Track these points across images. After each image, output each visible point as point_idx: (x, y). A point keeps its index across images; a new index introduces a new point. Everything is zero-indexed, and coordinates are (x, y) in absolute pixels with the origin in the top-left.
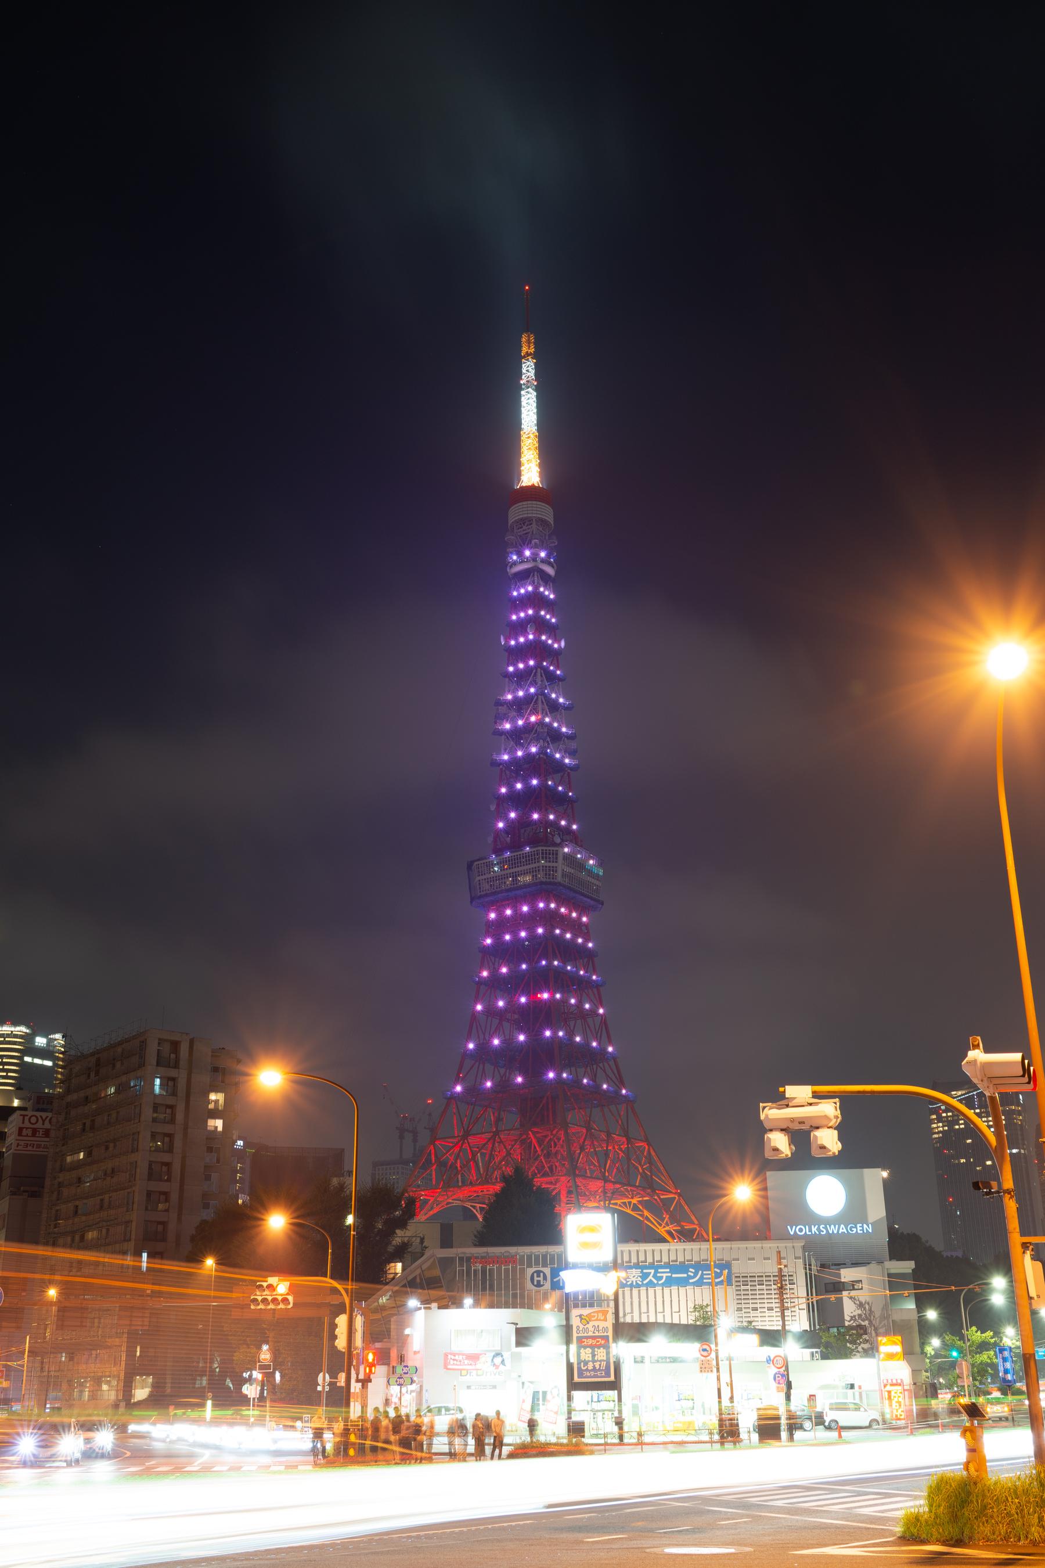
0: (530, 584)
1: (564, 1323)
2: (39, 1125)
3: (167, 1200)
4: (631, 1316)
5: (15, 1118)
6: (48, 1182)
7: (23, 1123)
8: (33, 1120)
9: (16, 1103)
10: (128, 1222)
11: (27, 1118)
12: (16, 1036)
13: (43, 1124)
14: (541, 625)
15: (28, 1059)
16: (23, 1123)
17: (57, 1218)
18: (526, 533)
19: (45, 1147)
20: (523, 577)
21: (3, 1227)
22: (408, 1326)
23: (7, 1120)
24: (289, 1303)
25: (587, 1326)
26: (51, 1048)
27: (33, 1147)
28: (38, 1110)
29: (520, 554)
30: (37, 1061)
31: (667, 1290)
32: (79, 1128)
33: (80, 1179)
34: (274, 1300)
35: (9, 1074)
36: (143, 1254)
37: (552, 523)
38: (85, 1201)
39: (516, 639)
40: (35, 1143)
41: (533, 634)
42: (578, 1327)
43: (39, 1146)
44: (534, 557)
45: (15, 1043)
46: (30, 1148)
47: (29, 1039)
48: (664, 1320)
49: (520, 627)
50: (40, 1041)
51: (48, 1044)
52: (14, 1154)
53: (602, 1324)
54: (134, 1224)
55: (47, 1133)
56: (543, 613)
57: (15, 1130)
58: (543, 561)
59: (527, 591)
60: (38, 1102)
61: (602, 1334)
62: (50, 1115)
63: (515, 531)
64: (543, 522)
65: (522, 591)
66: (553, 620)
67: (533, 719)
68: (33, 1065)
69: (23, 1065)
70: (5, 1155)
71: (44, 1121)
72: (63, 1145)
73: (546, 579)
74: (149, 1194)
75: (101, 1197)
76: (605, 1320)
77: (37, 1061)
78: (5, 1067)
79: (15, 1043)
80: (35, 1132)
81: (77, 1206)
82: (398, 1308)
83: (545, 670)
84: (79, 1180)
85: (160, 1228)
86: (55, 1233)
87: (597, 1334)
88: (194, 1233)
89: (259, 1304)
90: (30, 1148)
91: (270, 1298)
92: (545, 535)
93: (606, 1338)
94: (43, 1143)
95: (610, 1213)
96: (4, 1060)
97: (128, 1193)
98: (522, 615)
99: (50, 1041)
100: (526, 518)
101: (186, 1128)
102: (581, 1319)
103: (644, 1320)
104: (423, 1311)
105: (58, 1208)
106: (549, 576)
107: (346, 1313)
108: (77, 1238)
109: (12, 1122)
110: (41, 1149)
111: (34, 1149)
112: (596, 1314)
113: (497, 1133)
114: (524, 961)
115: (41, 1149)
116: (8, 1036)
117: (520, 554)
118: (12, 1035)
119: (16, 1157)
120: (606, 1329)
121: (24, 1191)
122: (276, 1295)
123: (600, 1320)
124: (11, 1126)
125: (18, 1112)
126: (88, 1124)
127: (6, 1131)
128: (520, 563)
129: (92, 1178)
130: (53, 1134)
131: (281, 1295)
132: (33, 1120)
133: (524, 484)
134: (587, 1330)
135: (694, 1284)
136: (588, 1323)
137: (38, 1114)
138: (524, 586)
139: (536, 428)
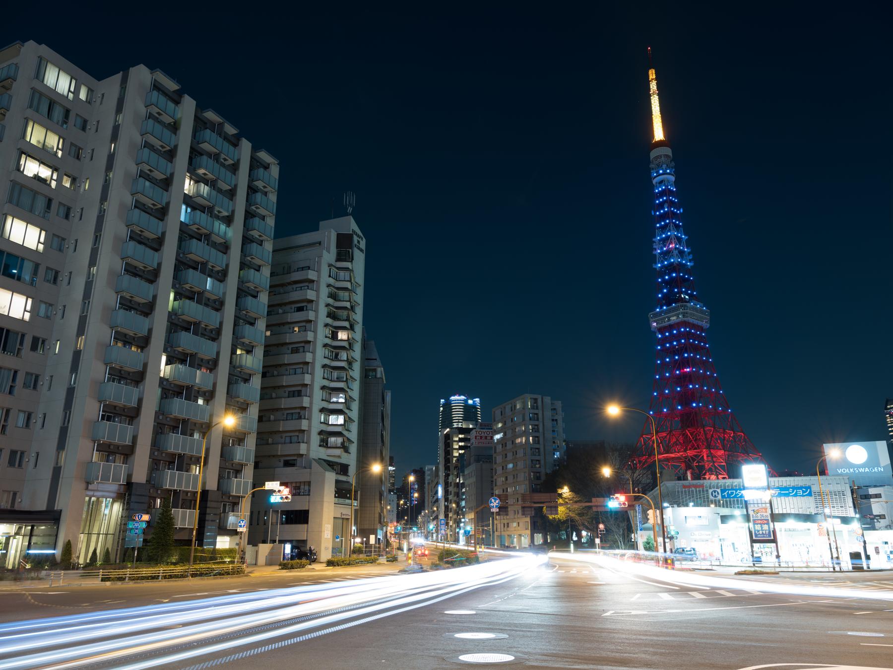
1: (745, 513)
2: (483, 434)
3: (539, 464)
5: (473, 433)
8: (480, 433)
9: (471, 426)
14: (672, 204)
19: (486, 443)
23: (470, 433)
31: (779, 499)
46: (480, 444)
49: (661, 205)
53: (765, 514)
55: (486, 438)
60: (481, 426)
74: (532, 460)
76: (766, 512)
80: (481, 437)
83: (675, 223)
87: (763, 518)
93: (768, 520)
95: (741, 466)
101: (544, 434)
102: (754, 512)
104: (670, 508)
107: (652, 509)
113: (671, 431)
114: (677, 355)
120: (767, 516)
125: (474, 430)
127: (469, 437)
132: (480, 433)
137: (482, 430)
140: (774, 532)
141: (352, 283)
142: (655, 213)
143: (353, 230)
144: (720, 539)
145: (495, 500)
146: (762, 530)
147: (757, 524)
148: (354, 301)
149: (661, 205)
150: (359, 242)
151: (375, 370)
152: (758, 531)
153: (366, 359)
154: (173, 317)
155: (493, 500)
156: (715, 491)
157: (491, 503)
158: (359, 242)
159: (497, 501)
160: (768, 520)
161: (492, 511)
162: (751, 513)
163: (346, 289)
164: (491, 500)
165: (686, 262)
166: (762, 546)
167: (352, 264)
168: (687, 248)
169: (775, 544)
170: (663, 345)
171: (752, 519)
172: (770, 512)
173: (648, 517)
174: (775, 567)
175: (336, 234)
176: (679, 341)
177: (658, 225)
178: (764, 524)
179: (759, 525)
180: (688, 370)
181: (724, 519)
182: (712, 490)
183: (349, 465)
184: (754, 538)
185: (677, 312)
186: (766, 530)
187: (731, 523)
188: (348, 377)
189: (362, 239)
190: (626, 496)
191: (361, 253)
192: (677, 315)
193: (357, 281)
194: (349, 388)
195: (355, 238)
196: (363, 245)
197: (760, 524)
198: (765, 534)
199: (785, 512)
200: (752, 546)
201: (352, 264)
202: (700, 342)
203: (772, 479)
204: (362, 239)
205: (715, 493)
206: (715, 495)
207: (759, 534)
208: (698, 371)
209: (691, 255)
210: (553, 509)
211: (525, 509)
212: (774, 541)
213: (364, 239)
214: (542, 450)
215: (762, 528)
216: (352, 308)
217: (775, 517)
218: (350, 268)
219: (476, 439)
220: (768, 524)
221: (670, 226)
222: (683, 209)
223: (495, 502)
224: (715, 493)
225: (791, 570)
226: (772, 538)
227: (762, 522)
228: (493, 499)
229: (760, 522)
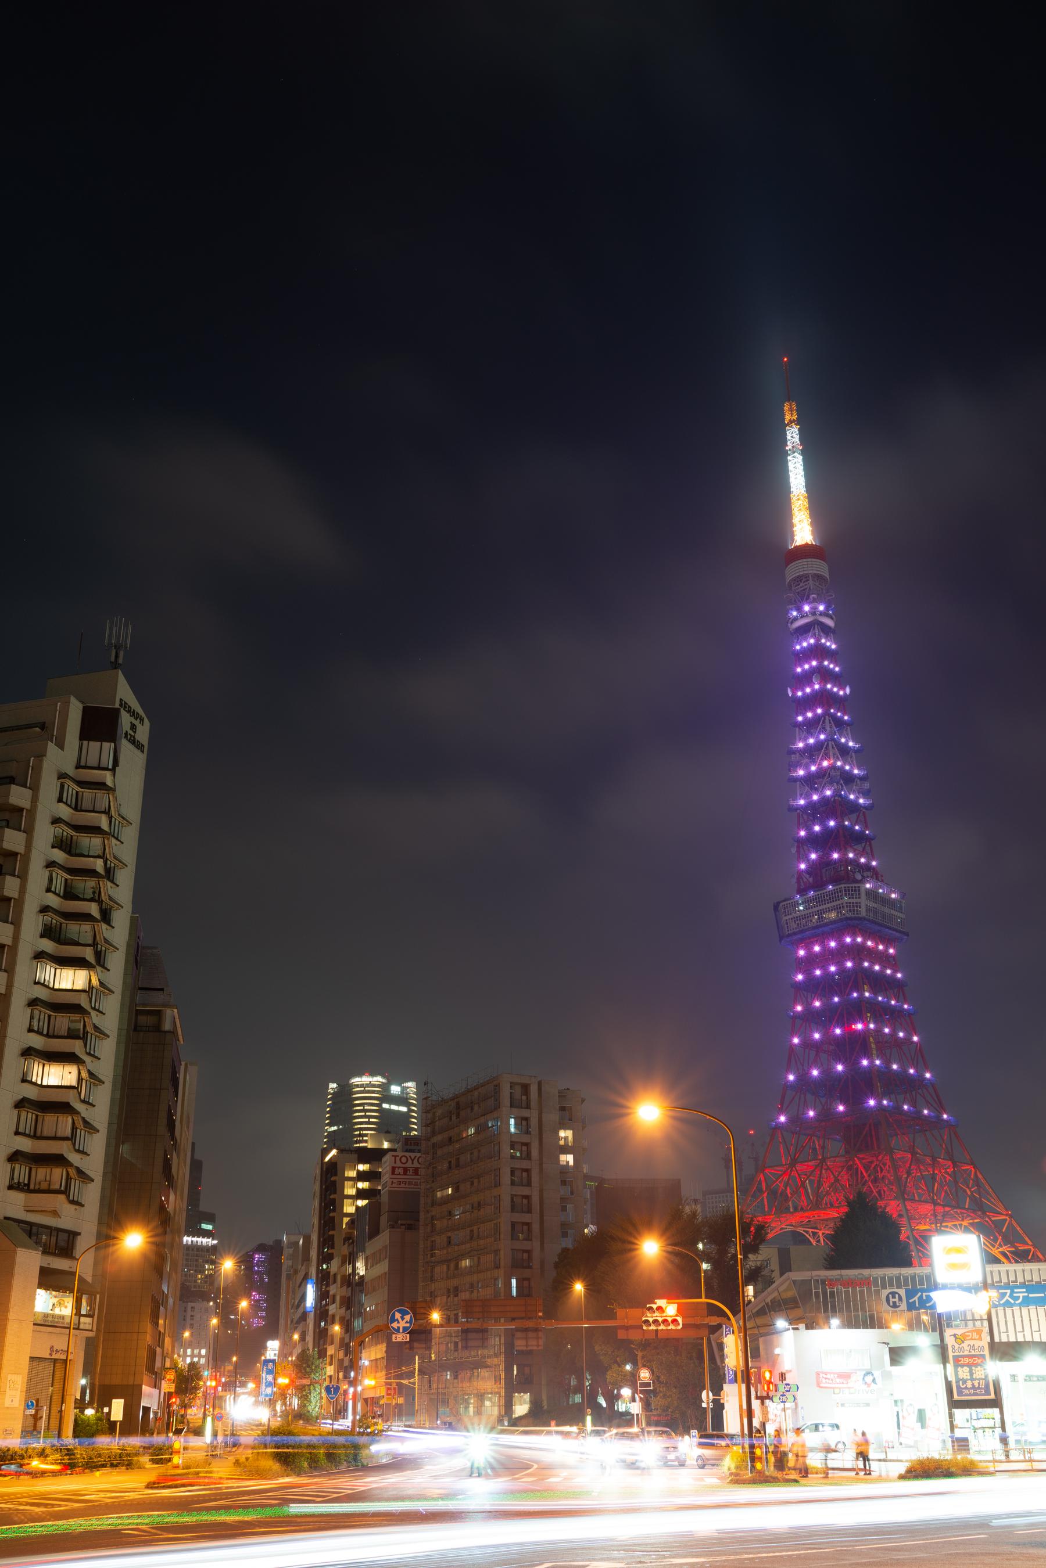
0: (812, 637)
2: (409, 1164)
4: (1002, 1336)
5: (387, 1159)
6: (422, 1215)
7: (395, 1163)
8: (404, 1160)
9: (386, 1145)
10: (496, 1252)
11: (398, 1158)
12: (374, 1086)
13: (413, 1163)
14: (825, 675)
15: (385, 1106)
16: (395, 1163)
17: (433, 1248)
18: (804, 590)
19: (416, 1184)
20: (804, 631)
21: (386, 1257)
22: (778, 1346)
23: (381, 1161)
24: (679, 1324)
25: (962, 1345)
26: (405, 1096)
27: (405, 1184)
28: (407, 1151)
29: (799, 609)
30: (394, 1107)
32: (446, 1166)
33: (450, 1212)
34: (665, 1321)
35: (371, 1120)
36: (512, 1280)
37: (828, 578)
38: (456, 1233)
39: (803, 690)
40: (407, 1181)
41: (819, 684)
43: (410, 1183)
44: (814, 611)
45: (373, 1092)
46: (402, 1185)
47: (385, 1087)
48: (1016, 1338)
49: (806, 679)
50: (395, 1089)
51: (402, 1092)
52: (390, 1192)
53: (977, 1343)
54: (502, 1252)
55: (416, 1171)
56: (826, 663)
58: (821, 614)
59: (809, 644)
61: (978, 1353)
62: (419, 1155)
63: (793, 588)
64: (819, 578)
65: (805, 644)
66: (837, 669)
68: (389, 1110)
69: (382, 1111)
70: (382, 1192)
71: (413, 1160)
72: (433, 1182)
73: (826, 631)
75: (471, 1228)
76: (980, 1339)
77: (394, 1107)
78: (367, 1114)
79: (373, 1092)
80: (406, 1170)
81: (450, 1237)
82: (769, 1330)
83: (834, 717)
84: (450, 1214)
85: (525, 1255)
86: (432, 1262)
87: (973, 1353)
88: (557, 1260)
89: (650, 1325)
90: (402, 1185)
92: (822, 589)
94: (414, 1181)
96: (366, 1108)
97: (495, 1224)
98: (807, 667)
99: (404, 1089)
100: (802, 576)
101: (541, 1164)
102: (956, 1339)
105: (433, 1239)
106: (829, 627)
108: (452, 1265)
109: (385, 1162)
110: (412, 1186)
111: (407, 1186)
112: (970, 1334)
115: (412, 1186)
116: (368, 1085)
117: (799, 609)
118: (370, 1085)
119: (391, 1193)
121: (402, 1225)
122: (666, 1316)
123: (975, 1339)
124: (384, 1166)
125: (390, 1154)
126: (453, 1162)
127: (380, 1170)
128: (801, 618)
129: (461, 1211)
130: (422, 1172)
131: (671, 1317)
134: (962, 1349)
136: (963, 1342)
137: (407, 1154)
138: (805, 640)
139: (805, 489)
142: (794, 693)
143: (121, 700)
144: (896, 1402)
145: (404, 1313)
146: (972, 1380)
147: (962, 1366)
148: (115, 857)
149: (806, 679)
150: (133, 727)
151: (159, 1014)
152: (965, 1381)
153: (141, 989)
155: (398, 1315)
156: (893, 1294)
157: (393, 1320)
158: (133, 727)
159: (407, 1318)
160: (983, 1356)
161: (394, 1340)
162: (949, 1341)
163: (96, 830)
164: (394, 1314)
165: (857, 798)
166: (974, 1416)
167: (114, 775)
168: (859, 769)
169: (996, 1411)
170: (808, 973)
171: (951, 1355)
173: (726, 1351)
174: (995, 1461)
175: (80, 706)
176: (840, 964)
177: (800, 718)
178: (976, 1365)
179: (966, 1369)
180: (860, 1026)
181: (896, 1355)
182: (888, 1291)
183: (79, 1234)
184: (956, 1397)
185: (838, 903)
186: (979, 1379)
187: (911, 1364)
188: (90, 1029)
189: (142, 721)
190: (678, 1303)
191: (138, 752)
192: (838, 909)
193: (123, 812)
194: (89, 1054)
195: (125, 719)
196: (143, 733)
197: (969, 1365)
198: (979, 1388)
199: (1020, 1339)
200: (951, 1416)
201: (114, 775)
202: (884, 968)
203: (989, 1268)
204: (142, 721)
205: (894, 1297)
206: (894, 1303)
207: (966, 1388)
208: (878, 1031)
210: (530, 1334)
211: (471, 1335)
212: (996, 1403)
213: (146, 720)
215: (971, 1374)
216: (109, 874)
218: (109, 783)
219: (393, 1173)
221: (824, 722)
222: (850, 688)
223: (403, 1319)
224: (894, 1297)
226: (992, 1396)
227: (971, 1361)
228: (399, 1311)
229: (967, 1360)
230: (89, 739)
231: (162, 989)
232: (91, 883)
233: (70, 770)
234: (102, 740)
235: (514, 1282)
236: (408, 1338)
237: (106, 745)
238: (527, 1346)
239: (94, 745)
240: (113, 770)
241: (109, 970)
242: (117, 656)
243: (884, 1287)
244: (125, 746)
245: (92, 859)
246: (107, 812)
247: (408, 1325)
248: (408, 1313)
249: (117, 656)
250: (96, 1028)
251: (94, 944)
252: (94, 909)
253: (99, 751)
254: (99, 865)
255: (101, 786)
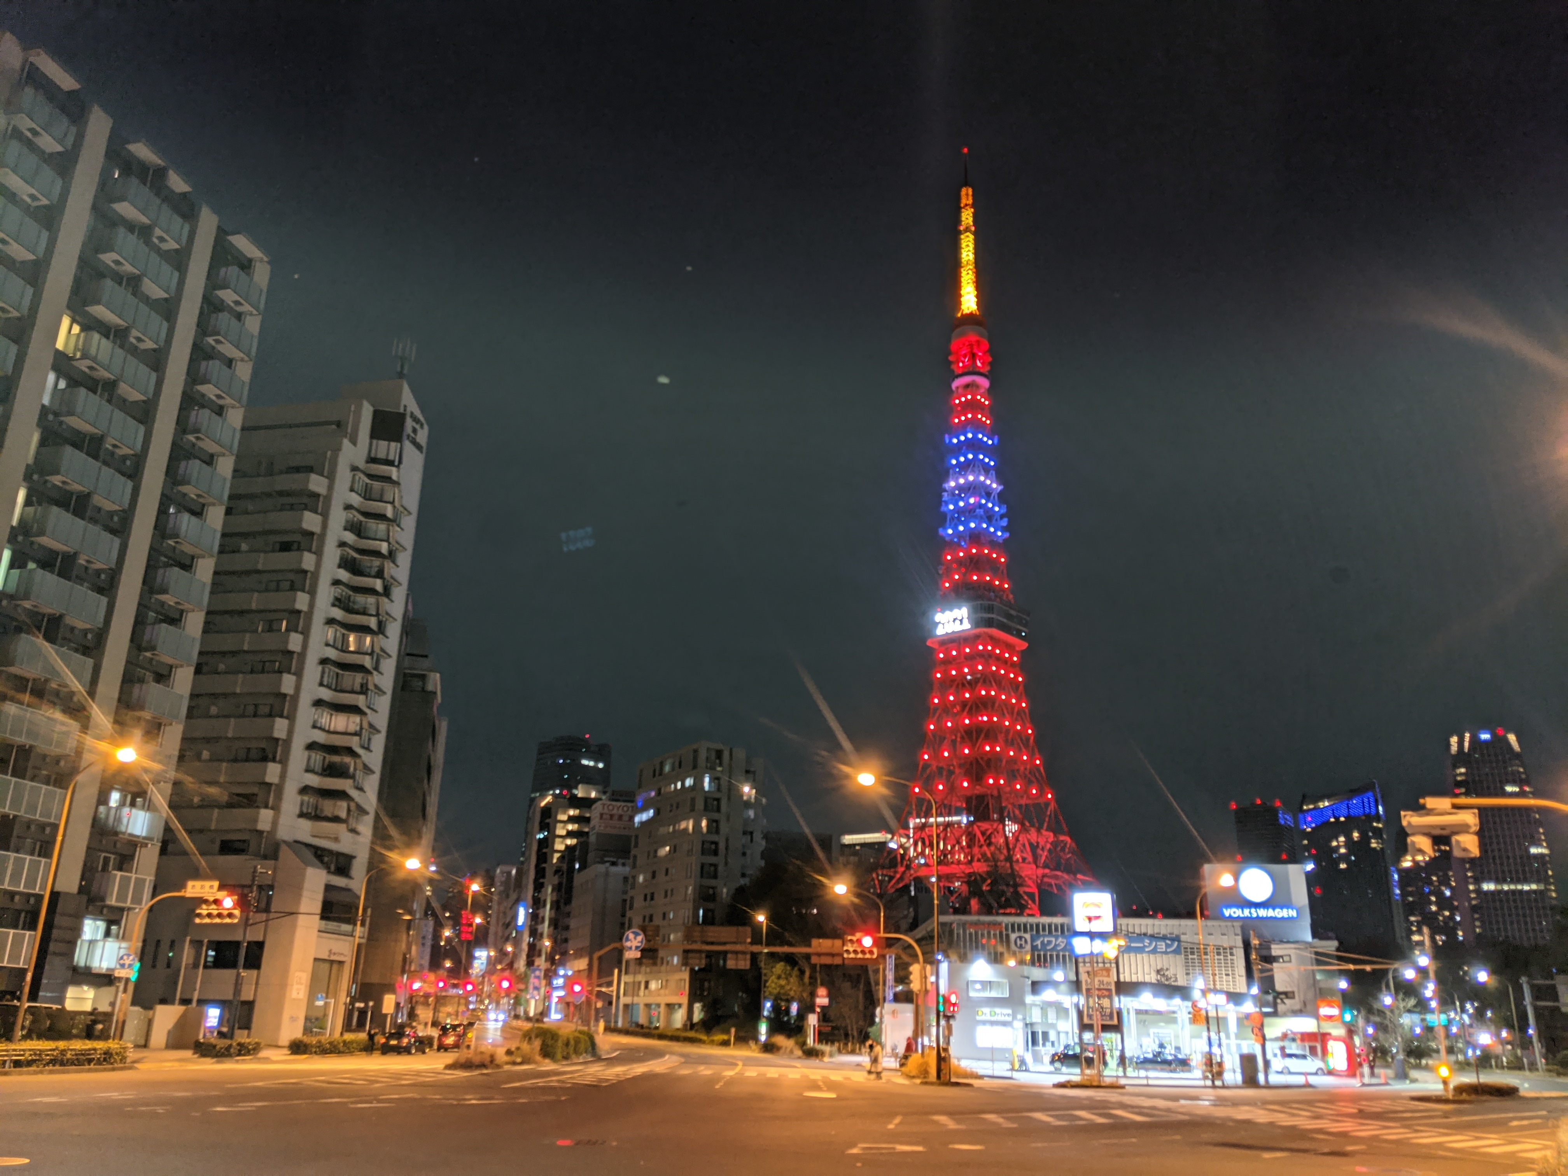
31: (1126, 956)
42: (1086, 981)
53: (1106, 980)
57: (598, 815)
67: (972, 501)
74: (702, 866)
76: (1108, 976)
87: (1102, 987)
91: (859, 950)
93: (1110, 990)
103: (1134, 979)
120: (1109, 983)
133: (966, 311)
135: (1149, 952)
140: (1119, 1014)
141: (394, 507)
145: (636, 934)
150: (415, 431)
151: (423, 677)
153: (408, 655)
154: (51, 417)
155: (631, 936)
157: (627, 939)
158: (415, 431)
159: (640, 938)
162: (1083, 977)
163: (382, 517)
171: (1084, 987)
172: (1115, 979)
174: (1117, 1077)
175: (371, 409)
178: (1104, 997)
188: (371, 687)
189: (422, 426)
191: (417, 452)
193: (405, 503)
194: (369, 707)
195: (409, 423)
196: (422, 437)
201: (398, 471)
204: (422, 426)
209: (1006, 520)
210: (740, 956)
211: (690, 955)
213: (426, 427)
214: (722, 846)
216: (391, 556)
217: (1125, 988)
218: (394, 477)
220: (1110, 997)
223: (635, 938)
225: (1144, 1082)
226: (1115, 1022)
228: (633, 933)
230: (379, 438)
231: (426, 656)
232: (377, 562)
233: (361, 464)
234: (390, 439)
235: (701, 912)
236: (638, 955)
237: (393, 444)
238: (736, 965)
239: (383, 444)
240: (398, 466)
241: (387, 637)
242: (402, 367)
243: (1013, 931)
244: (408, 445)
245: (378, 542)
246: (392, 503)
247: (639, 944)
248: (639, 934)
249: (402, 367)
250: (376, 687)
251: (377, 615)
252: (378, 585)
253: (383, 448)
254: (384, 548)
255: (388, 479)
